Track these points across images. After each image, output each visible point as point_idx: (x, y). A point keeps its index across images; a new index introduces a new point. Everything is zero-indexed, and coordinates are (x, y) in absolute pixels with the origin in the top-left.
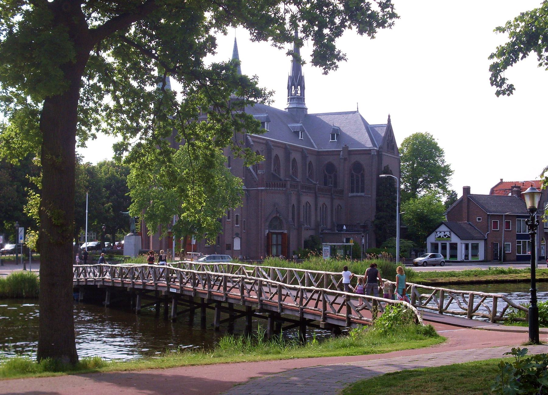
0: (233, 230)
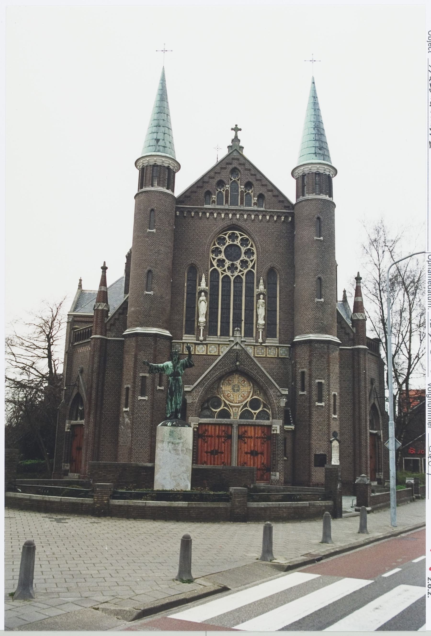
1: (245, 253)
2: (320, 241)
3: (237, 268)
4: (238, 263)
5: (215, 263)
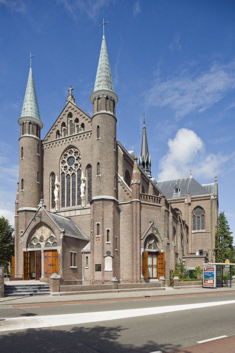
0: (103, 248)
1: (77, 160)
3: (73, 169)
4: (73, 166)
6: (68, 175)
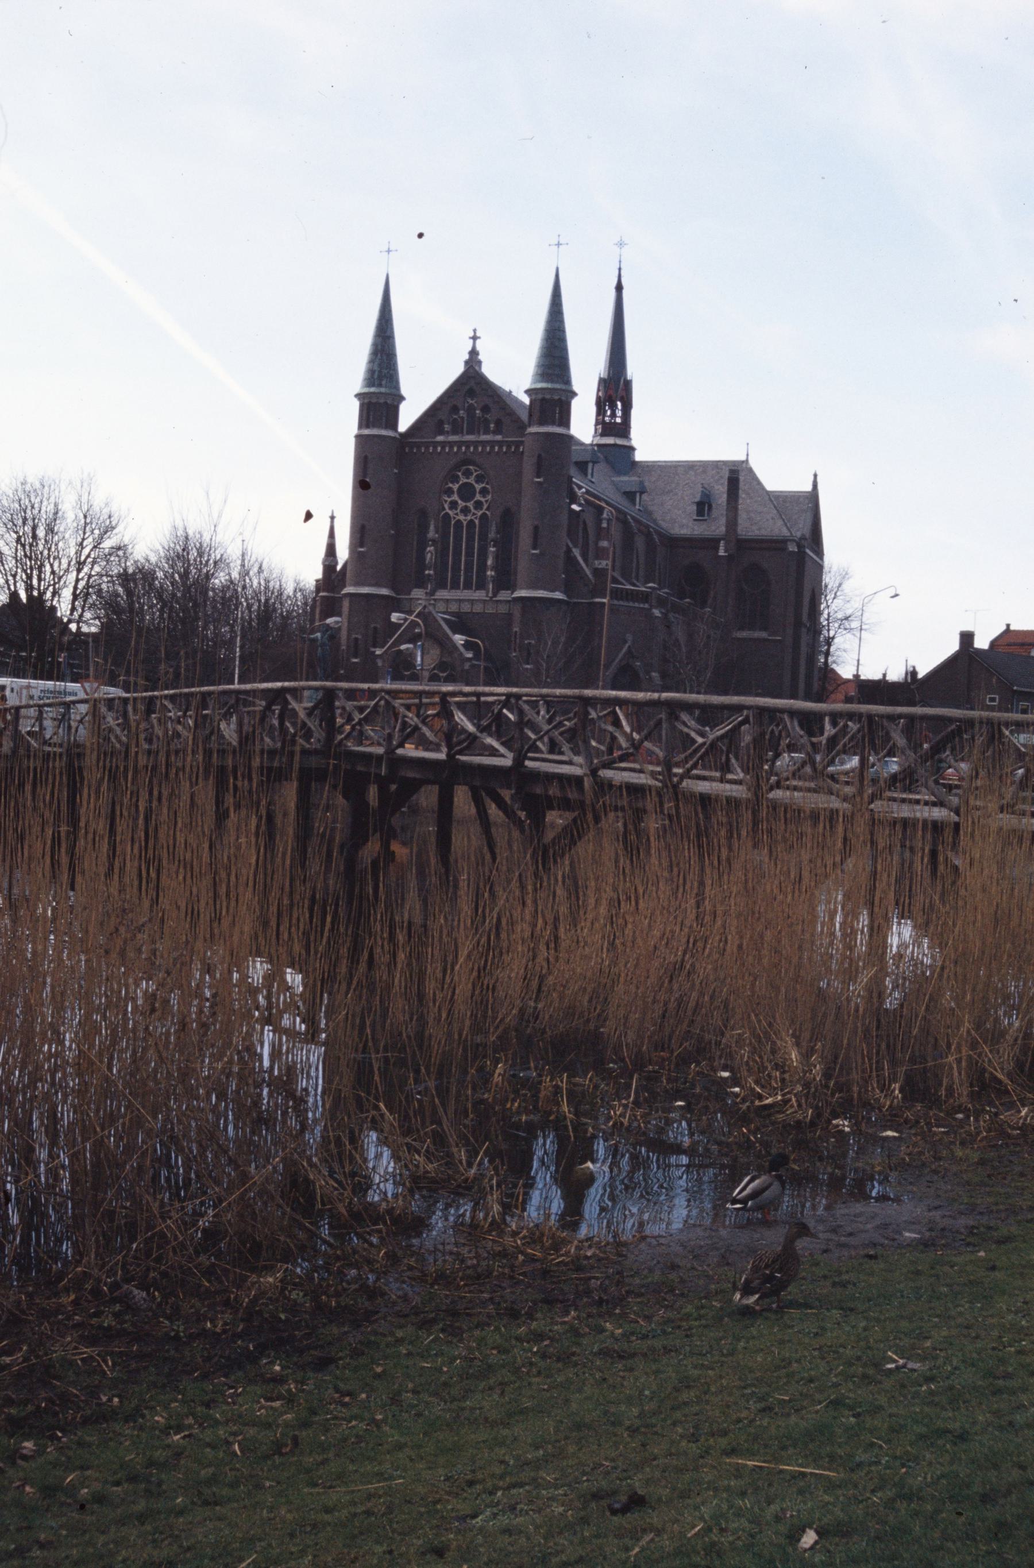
1: (480, 492)
2: (539, 483)
3: (470, 511)
4: (470, 505)
5: (446, 506)
6: (459, 521)
